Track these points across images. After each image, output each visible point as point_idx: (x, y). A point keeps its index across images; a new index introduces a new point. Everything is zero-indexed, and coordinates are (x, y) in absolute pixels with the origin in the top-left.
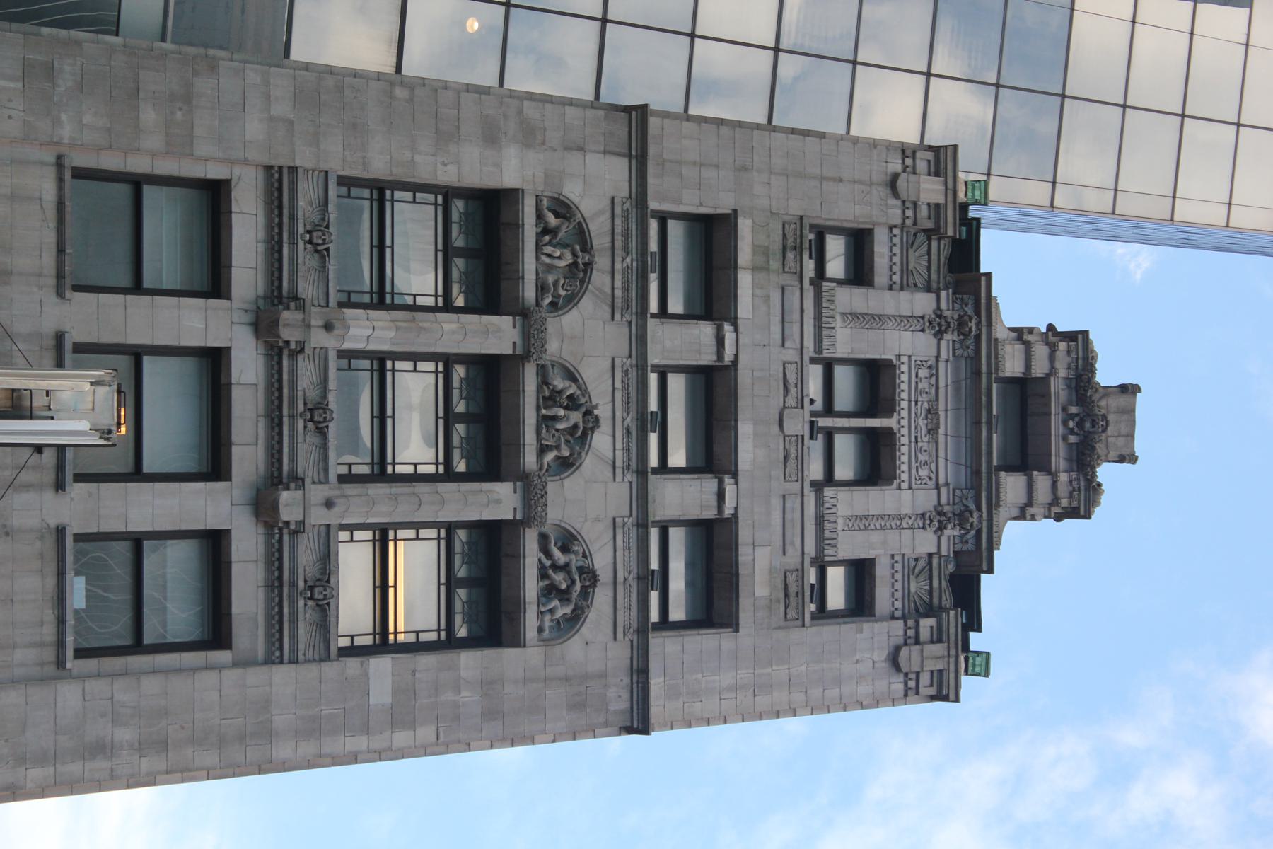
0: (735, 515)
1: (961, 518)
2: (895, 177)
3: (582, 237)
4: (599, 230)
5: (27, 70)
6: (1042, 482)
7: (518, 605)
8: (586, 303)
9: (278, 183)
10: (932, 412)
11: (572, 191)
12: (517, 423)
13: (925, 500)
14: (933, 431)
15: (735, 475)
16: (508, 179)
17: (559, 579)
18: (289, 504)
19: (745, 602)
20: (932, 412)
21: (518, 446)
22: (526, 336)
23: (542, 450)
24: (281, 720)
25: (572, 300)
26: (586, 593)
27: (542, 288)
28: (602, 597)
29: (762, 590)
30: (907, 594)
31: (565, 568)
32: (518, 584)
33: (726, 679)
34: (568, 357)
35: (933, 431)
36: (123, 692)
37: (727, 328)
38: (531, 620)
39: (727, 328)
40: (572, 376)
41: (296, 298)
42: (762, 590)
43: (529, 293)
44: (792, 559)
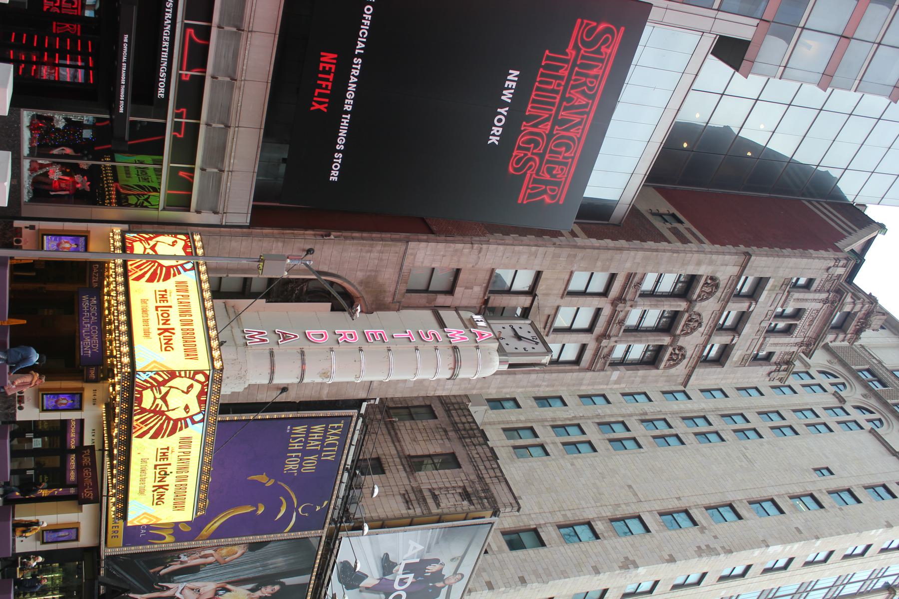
0: (734, 345)
1: (807, 345)
2: (830, 268)
3: (717, 286)
4: (722, 284)
5: (569, 256)
6: (841, 336)
7: (661, 361)
8: (711, 299)
9: (630, 276)
10: (812, 321)
11: (718, 275)
12: (679, 323)
13: (799, 340)
14: (810, 325)
15: (739, 335)
16: (699, 273)
17: (674, 357)
18: (604, 342)
19: (729, 362)
20: (812, 321)
21: (676, 329)
22: (689, 307)
23: (682, 330)
24: (585, 382)
25: (707, 299)
26: (681, 360)
27: (699, 296)
28: (685, 361)
29: (735, 359)
30: (783, 358)
31: (678, 355)
32: (663, 356)
33: (715, 377)
34: (700, 312)
35: (810, 325)
36: (547, 376)
37: (754, 303)
38: (662, 365)
39: (754, 303)
40: (699, 315)
41: (625, 300)
42: (735, 359)
43: (695, 297)
44: (749, 352)
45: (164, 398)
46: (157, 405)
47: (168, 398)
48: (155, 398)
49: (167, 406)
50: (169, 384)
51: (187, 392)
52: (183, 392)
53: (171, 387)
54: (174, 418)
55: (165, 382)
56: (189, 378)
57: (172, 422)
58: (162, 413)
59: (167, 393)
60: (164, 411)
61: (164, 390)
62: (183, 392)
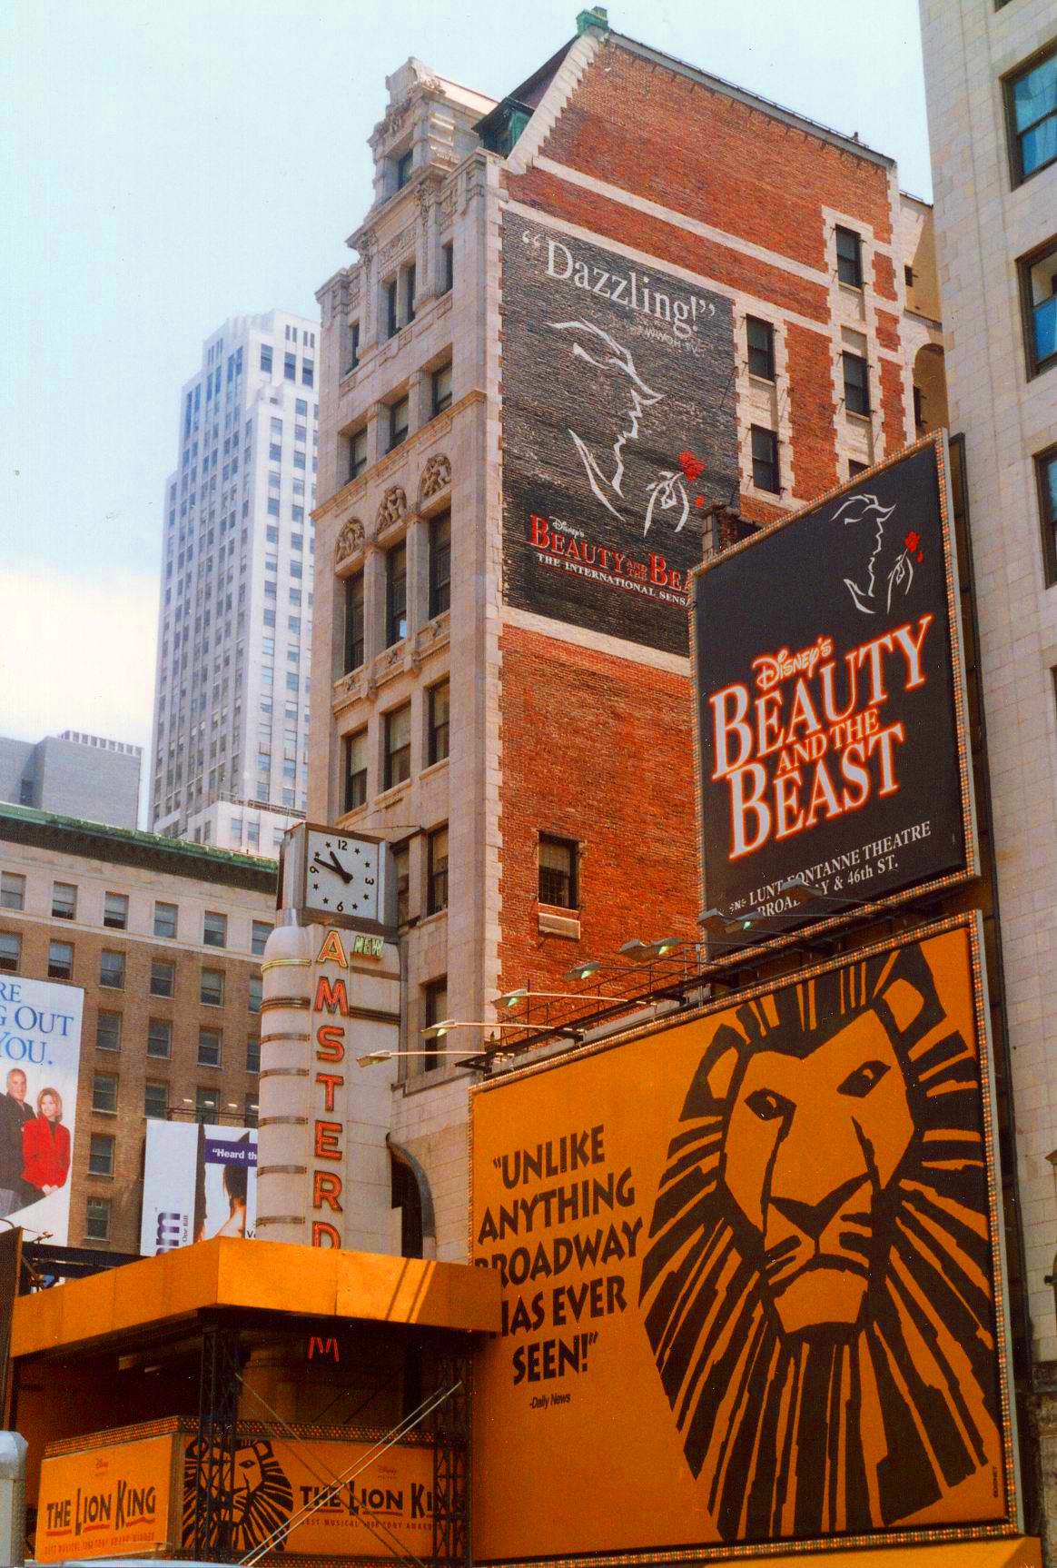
45: (810, 1218)
46: (848, 1240)
47: (813, 1196)
48: (820, 1261)
49: (850, 1188)
50: (752, 1211)
51: (785, 1109)
52: (783, 1133)
53: (767, 1198)
54: (909, 1128)
55: (748, 1239)
56: (724, 1127)
57: (931, 1136)
58: (888, 1201)
59: (791, 1208)
60: (876, 1199)
61: (779, 1228)
62: (783, 1133)
